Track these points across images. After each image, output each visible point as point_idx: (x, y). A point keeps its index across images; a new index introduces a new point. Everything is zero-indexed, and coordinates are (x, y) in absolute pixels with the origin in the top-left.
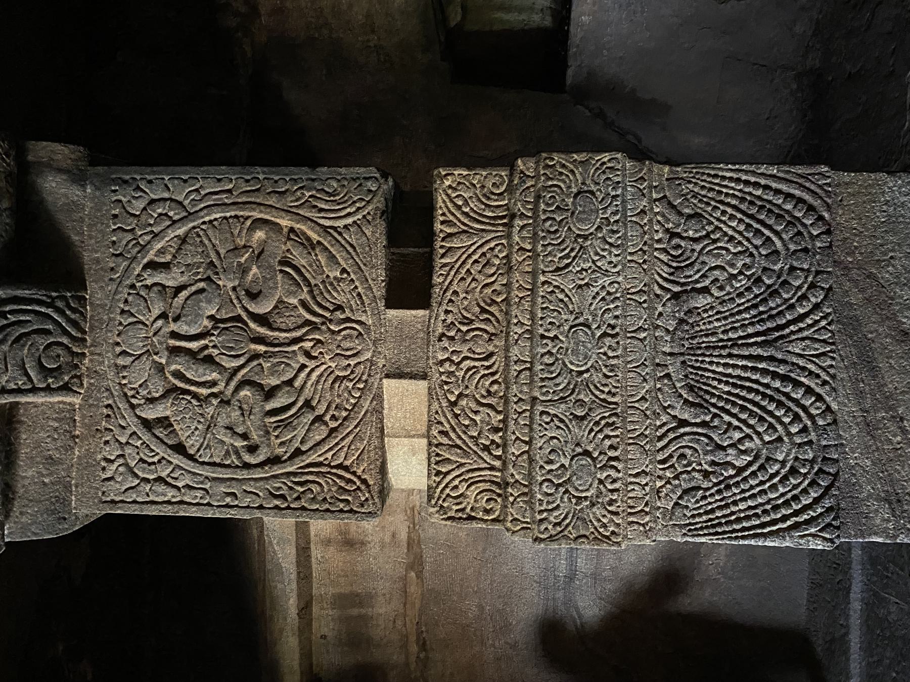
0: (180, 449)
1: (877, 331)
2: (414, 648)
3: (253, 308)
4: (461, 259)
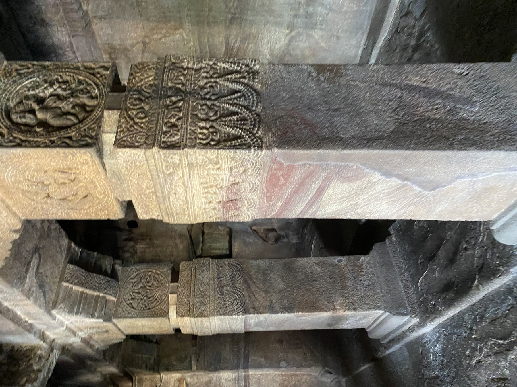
0: (133, 308)
1: (250, 282)
3: (148, 284)
4: (183, 275)
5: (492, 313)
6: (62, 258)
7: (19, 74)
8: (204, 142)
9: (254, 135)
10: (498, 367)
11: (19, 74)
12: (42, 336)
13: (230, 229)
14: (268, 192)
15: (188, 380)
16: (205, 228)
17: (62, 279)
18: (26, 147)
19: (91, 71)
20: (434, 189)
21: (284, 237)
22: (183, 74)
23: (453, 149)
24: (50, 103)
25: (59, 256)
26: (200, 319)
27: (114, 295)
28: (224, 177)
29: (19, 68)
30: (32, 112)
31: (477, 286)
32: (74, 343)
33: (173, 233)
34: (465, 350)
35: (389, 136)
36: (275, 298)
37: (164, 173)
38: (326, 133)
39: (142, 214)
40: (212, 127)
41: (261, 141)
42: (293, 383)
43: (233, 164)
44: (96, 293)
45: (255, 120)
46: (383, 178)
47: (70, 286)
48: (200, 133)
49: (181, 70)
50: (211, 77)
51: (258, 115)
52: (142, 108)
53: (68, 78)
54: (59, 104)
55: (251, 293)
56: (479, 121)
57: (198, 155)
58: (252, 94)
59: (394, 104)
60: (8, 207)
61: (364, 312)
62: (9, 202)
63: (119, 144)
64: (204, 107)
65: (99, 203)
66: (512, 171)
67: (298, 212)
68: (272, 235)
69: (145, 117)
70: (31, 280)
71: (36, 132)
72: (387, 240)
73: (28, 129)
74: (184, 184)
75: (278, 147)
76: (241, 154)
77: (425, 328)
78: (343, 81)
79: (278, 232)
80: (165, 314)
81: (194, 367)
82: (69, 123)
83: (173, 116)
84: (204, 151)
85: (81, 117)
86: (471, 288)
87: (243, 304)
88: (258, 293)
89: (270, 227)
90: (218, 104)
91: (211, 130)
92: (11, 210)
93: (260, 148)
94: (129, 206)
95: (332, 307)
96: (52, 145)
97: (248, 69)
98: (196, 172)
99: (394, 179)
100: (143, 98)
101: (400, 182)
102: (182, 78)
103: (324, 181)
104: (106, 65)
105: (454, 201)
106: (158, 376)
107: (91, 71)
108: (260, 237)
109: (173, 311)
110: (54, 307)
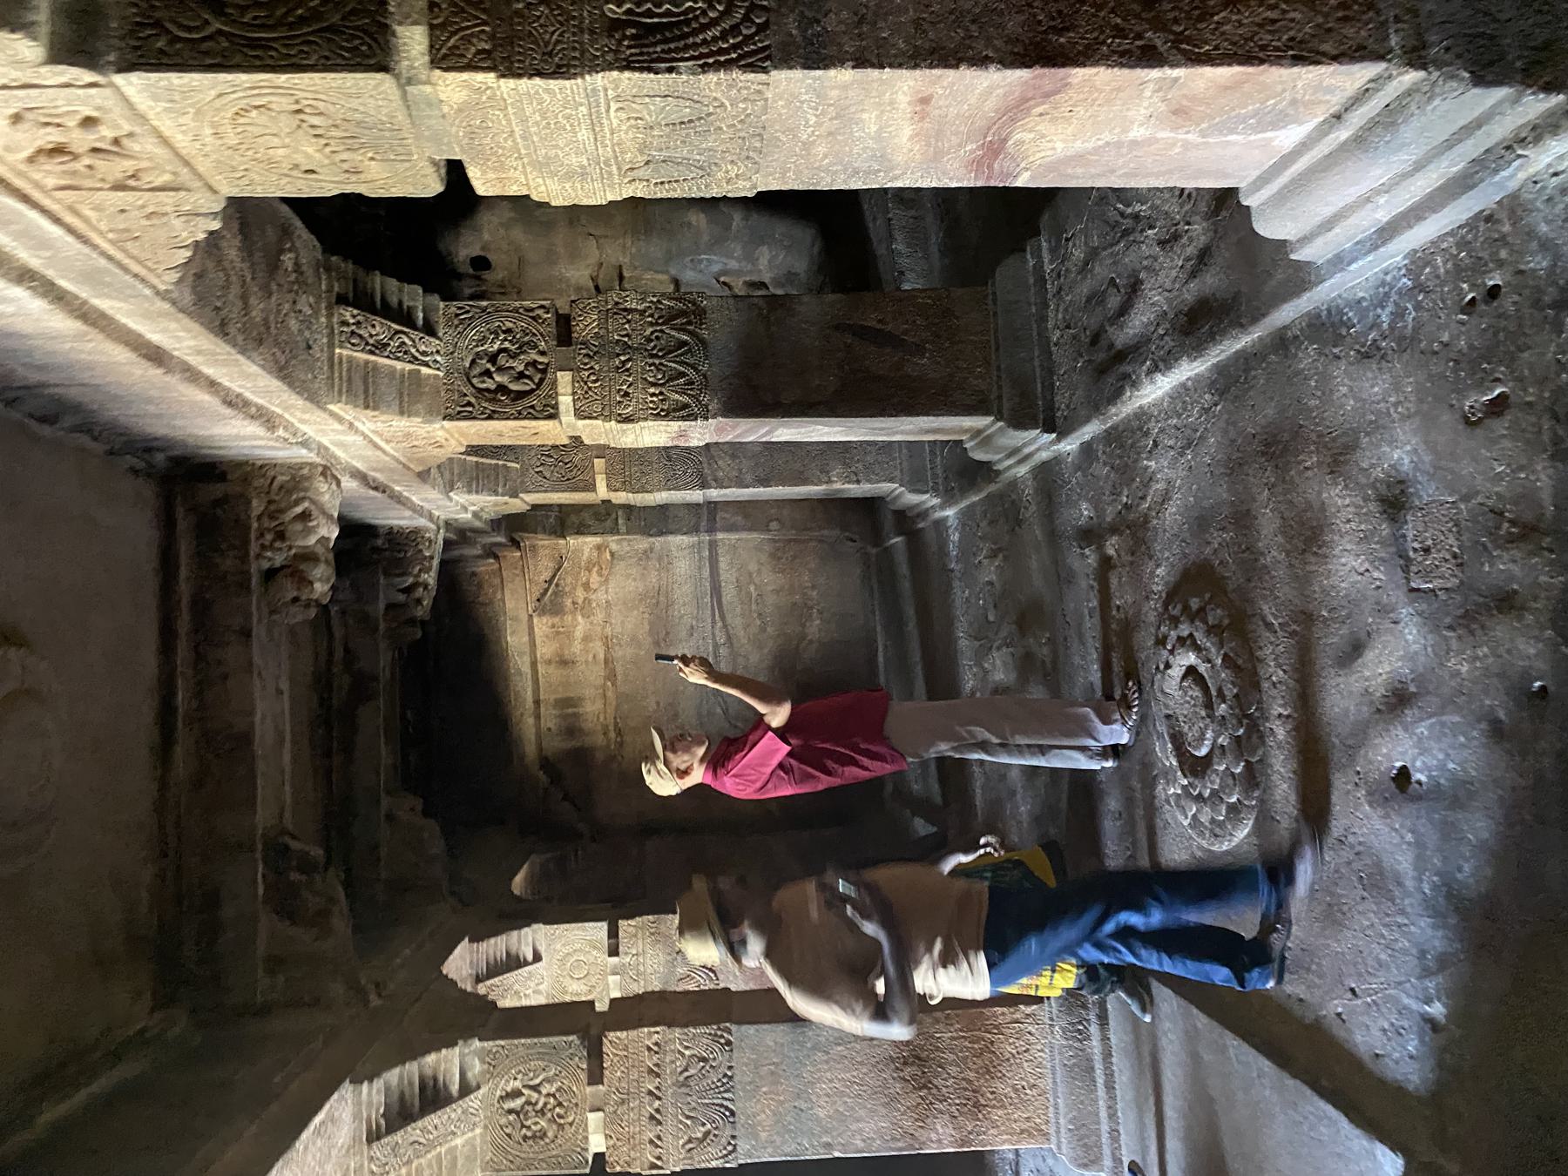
2: (612, 735)
15: (614, 547)
22: (629, 322)
75: (724, 416)
87: (701, 475)
89: (755, 278)
106: (562, 542)
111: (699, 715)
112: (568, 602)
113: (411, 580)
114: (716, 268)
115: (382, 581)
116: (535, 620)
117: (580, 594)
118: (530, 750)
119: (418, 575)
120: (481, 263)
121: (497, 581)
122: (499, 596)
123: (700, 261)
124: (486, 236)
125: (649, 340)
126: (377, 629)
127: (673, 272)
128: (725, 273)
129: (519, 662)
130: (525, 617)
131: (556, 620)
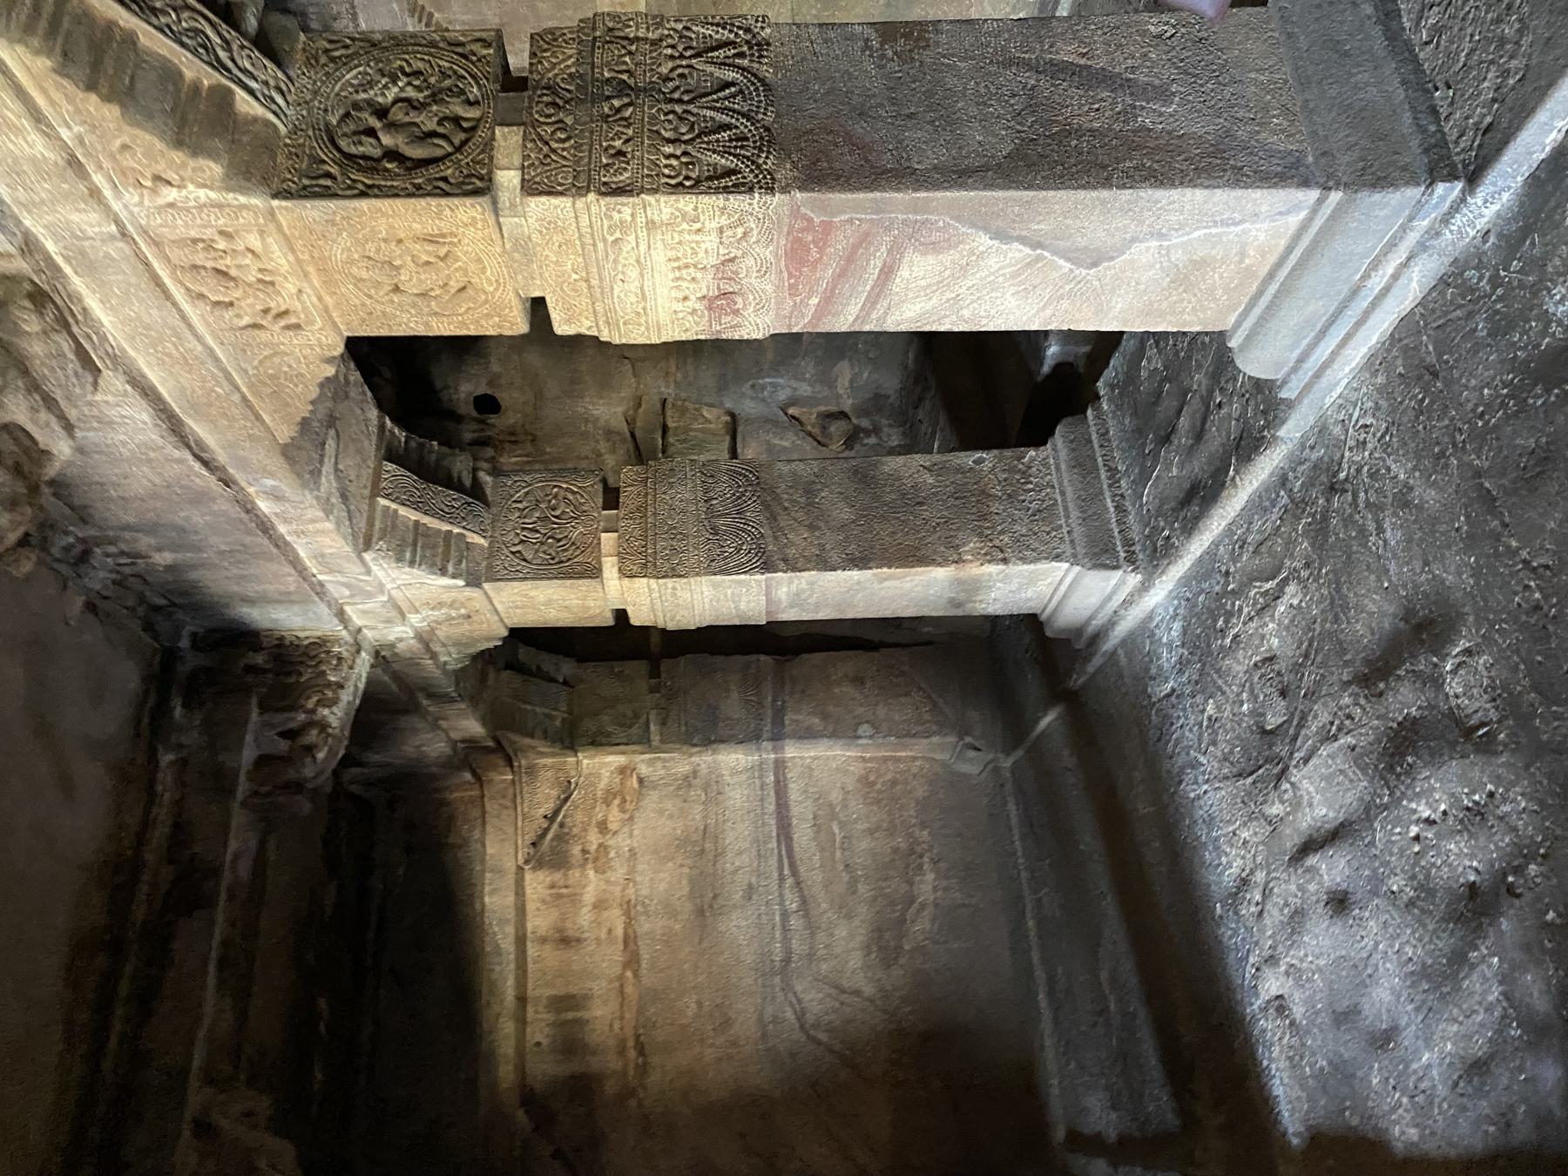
1: (778, 510)
2: (632, 1054)
4: (629, 497)
5: (1259, 532)
6: (370, 447)
7: (333, 59)
8: (673, 182)
9: (758, 167)
10: (1263, 637)
11: (333, 59)
12: (341, 615)
13: (733, 415)
14: (790, 276)
15: (644, 770)
16: (669, 413)
17: (376, 492)
18: (376, 196)
19: (460, 50)
20: (1095, 264)
21: (868, 433)
22: (630, 53)
23: (1111, 187)
24: (398, 115)
25: (366, 442)
26: (670, 582)
27: (482, 533)
28: (709, 248)
29: (328, 46)
30: (371, 132)
31: (1233, 479)
32: (400, 640)
33: (590, 425)
34: (1215, 621)
35: (999, 165)
36: (830, 539)
37: (605, 240)
38: (887, 161)
39: (562, 328)
40: (685, 153)
41: (773, 179)
42: (889, 776)
43: (724, 221)
44: (446, 527)
45: (762, 138)
46: (996, 243)
47: (394, 506)
48: (666, 166)
49: (625, 43)
50: (682, 56)
51: (767, 129)
52: (561, 121)
53: (421, 65)
54: (414, 117)
55: (777, 531)
56: (1169, 133)
57: (663, 206)
58: (757, 89)
59: (1018, 103)
60: (326, 309)
61: (1026, 567)
62: (329, 300)
63: (531, 188)
64: (671, 117)
65: (486, 301)
66: (1228, 225)
67: (851, 319)
68: (836, 428)
69: (569, 138)
70: (328, 482)
71: (387, 170)
72: (1089, 412)
73: (370, 165)
74: (638, 261)
75: (801, 188)
76: (736, 202)
77: (1152, 592)
78: (927, 56)
79: (855, 421)
80: (593, 572)
81: (655, 739)
82: (439, 153)
83: (618, 135)
84: (673, 197)
85: (457, 142)
86: (1223, 485)
87: (760, 551)
88: (794, 530)
89: (833, 408)
90: (696, 111)
91: (684, 160)
92: (330, 317)
93: (770, 190)
94: (538, 307)
95: (955, 557)
96: (418, 192)
97: (749, 37)
98: (659, 237)
99: (1016, 245)
100: (561, 103)
101: (1028, 251)
102: (627, 59)
103: (890, 251)
104: (484, 35)
105: (1142, 287)
106: (572, 759)
107: (460, 50)
108: (810, 434)
109: (610, 567)
110: (368, 546)
111: (761, 1019)
112: (576, 850)
113: (302, 717)
114: (783, 395)
115: (254, 716)
116: (528, 876)
117: (594, 838)
118: (506, 1073)
119: (313, 711)
120: (487, 404)
121: (476, 813)
122: (477, 834)
123: (763, 388)
124: (495, 367)
125: (667, 79)
126: (230, 792)
127: (728, 405)
128: (793, 402)
129: (501, 936)
130: (510, 866)
131: (558, 876)
